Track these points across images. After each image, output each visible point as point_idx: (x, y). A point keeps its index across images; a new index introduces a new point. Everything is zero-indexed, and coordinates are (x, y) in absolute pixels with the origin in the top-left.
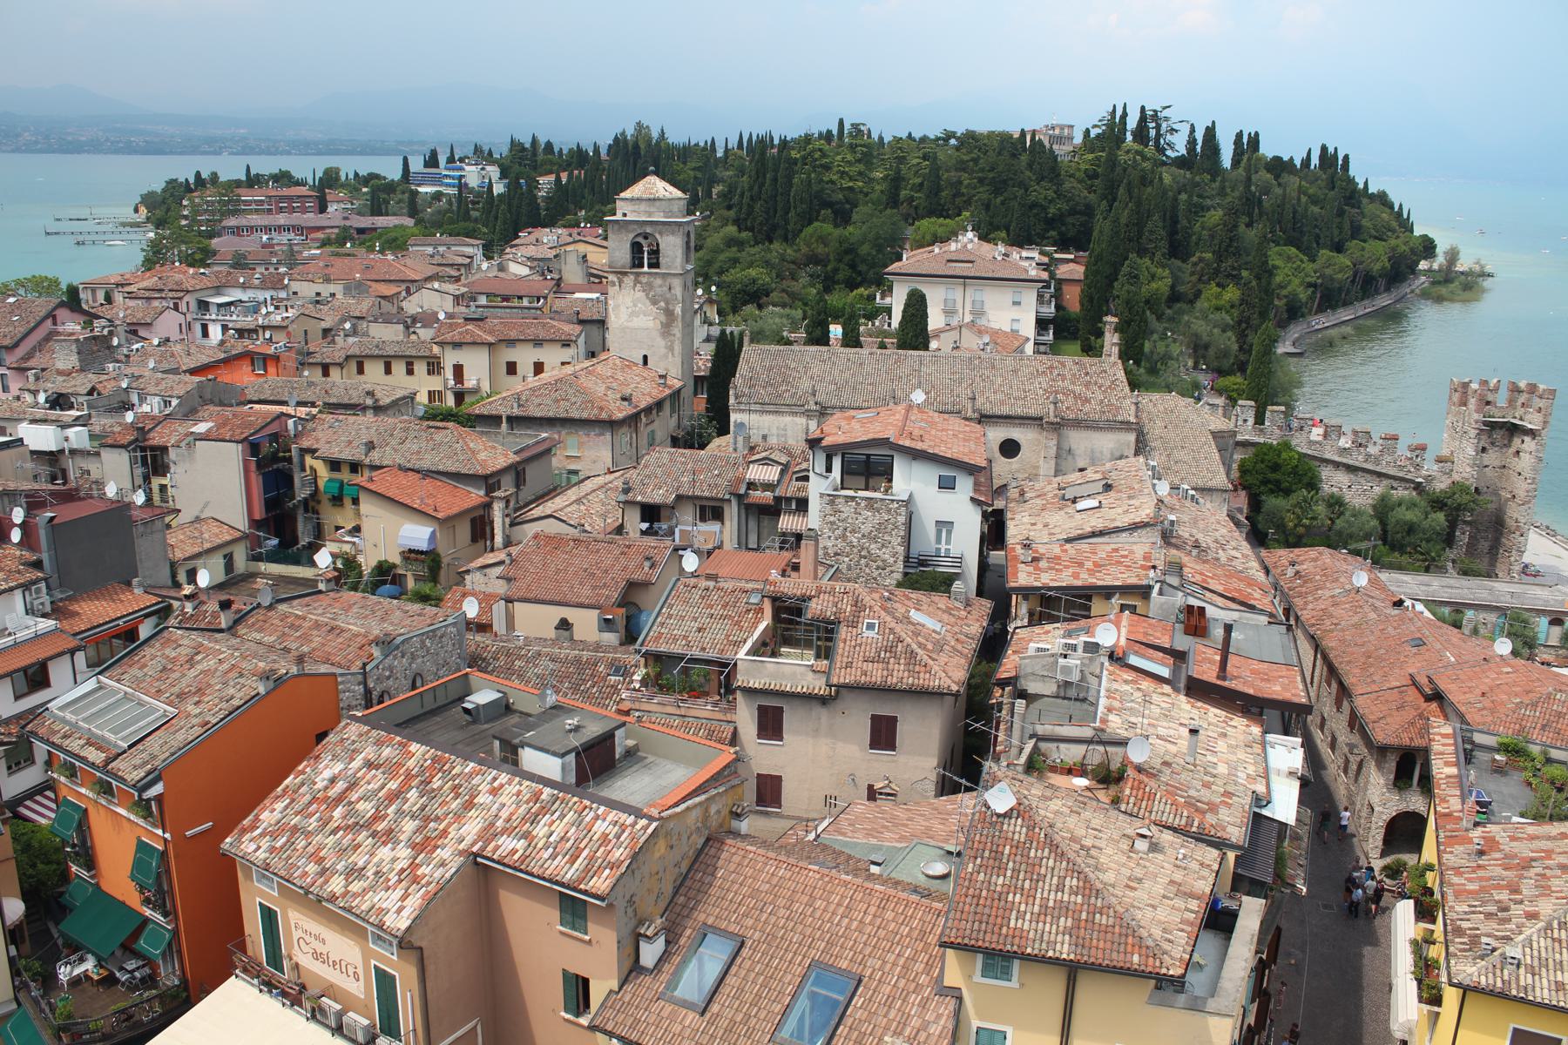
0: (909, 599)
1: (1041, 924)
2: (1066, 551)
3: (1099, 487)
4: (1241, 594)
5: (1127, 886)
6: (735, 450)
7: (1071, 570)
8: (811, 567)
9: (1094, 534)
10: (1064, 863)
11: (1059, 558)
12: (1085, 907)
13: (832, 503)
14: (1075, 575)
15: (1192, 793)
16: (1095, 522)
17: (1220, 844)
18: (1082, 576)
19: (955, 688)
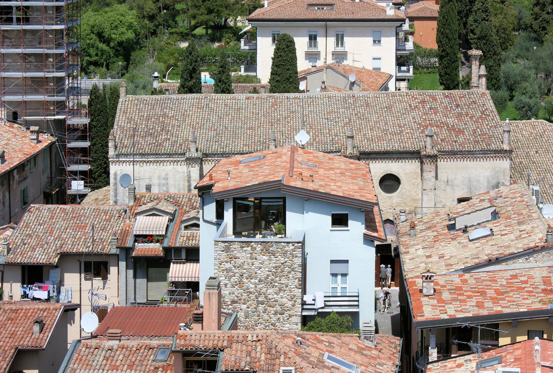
0: (321, 342)
3: (487, 215)
6: (116, 202)
7: (474, 300)
8: (215, 317)
9: (490, 262)
11: (460, 289)
13: (227, 249)
14: (480, 305)
18: (486, 305)
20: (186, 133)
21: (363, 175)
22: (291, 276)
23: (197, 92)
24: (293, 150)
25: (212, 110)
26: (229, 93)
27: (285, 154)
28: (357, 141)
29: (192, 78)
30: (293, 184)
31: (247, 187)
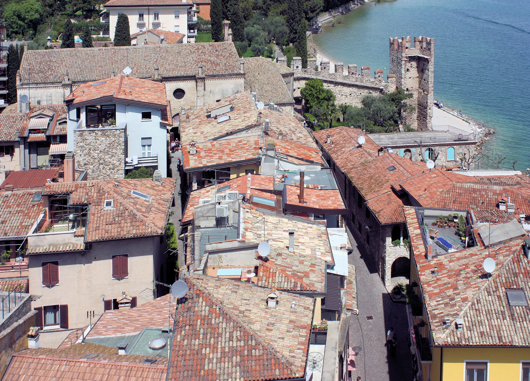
0: (130, 184)
1: (223, 363)
2: (214, 145)
4: (306, 156)
5: (268, 329)
6: (21, 111)
7: (218, 155)
8: (71, 174)
9: (227, 134)
10: (232, 323)
11: (210, 150)
12: (246, 347)
13: (81, 135)
14: (220, 158)
15: (294, 268)
16: (228, 128)
17: (312, 295)
18: (223, 158)
19: (160, 232)
20: (62, 70)
21: (161, 90)
22: (118, 148)
23: (72, 47)
24: (122, 78)
25: (78, 57)
26: (91, 47)
27: (117, 80)
28: (160, 72)
29: (69, 39)
30: (119, 97)
31: (93, 99)
